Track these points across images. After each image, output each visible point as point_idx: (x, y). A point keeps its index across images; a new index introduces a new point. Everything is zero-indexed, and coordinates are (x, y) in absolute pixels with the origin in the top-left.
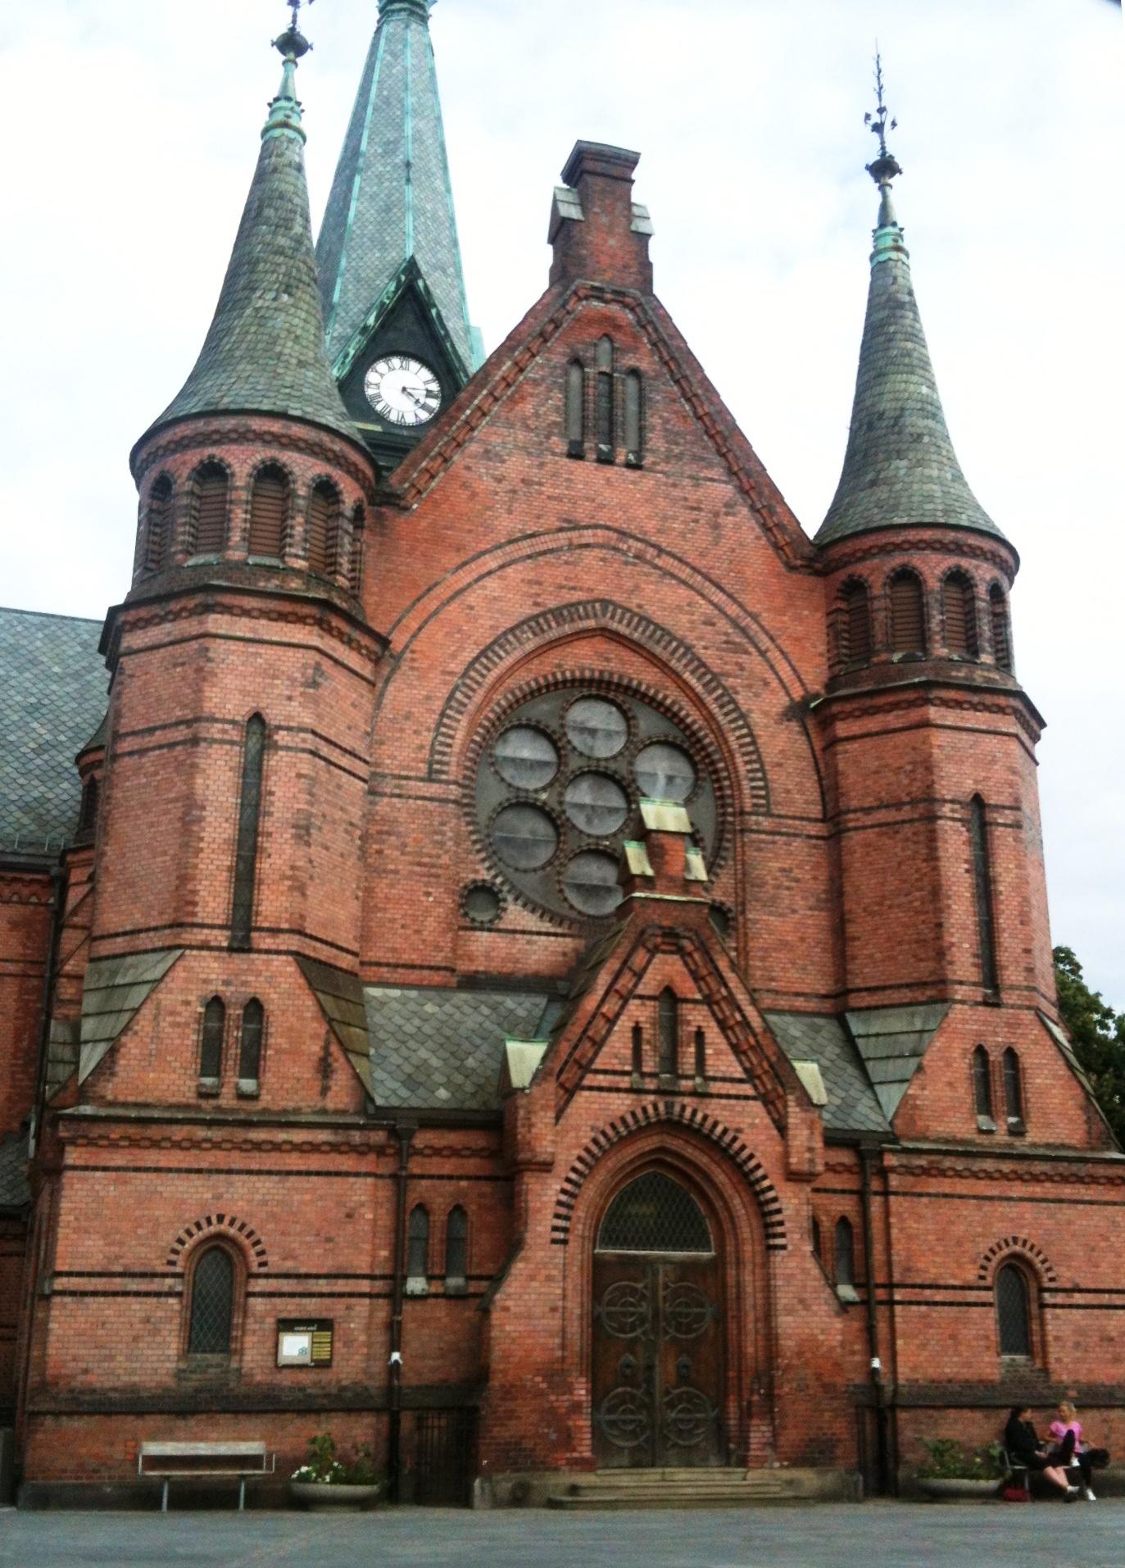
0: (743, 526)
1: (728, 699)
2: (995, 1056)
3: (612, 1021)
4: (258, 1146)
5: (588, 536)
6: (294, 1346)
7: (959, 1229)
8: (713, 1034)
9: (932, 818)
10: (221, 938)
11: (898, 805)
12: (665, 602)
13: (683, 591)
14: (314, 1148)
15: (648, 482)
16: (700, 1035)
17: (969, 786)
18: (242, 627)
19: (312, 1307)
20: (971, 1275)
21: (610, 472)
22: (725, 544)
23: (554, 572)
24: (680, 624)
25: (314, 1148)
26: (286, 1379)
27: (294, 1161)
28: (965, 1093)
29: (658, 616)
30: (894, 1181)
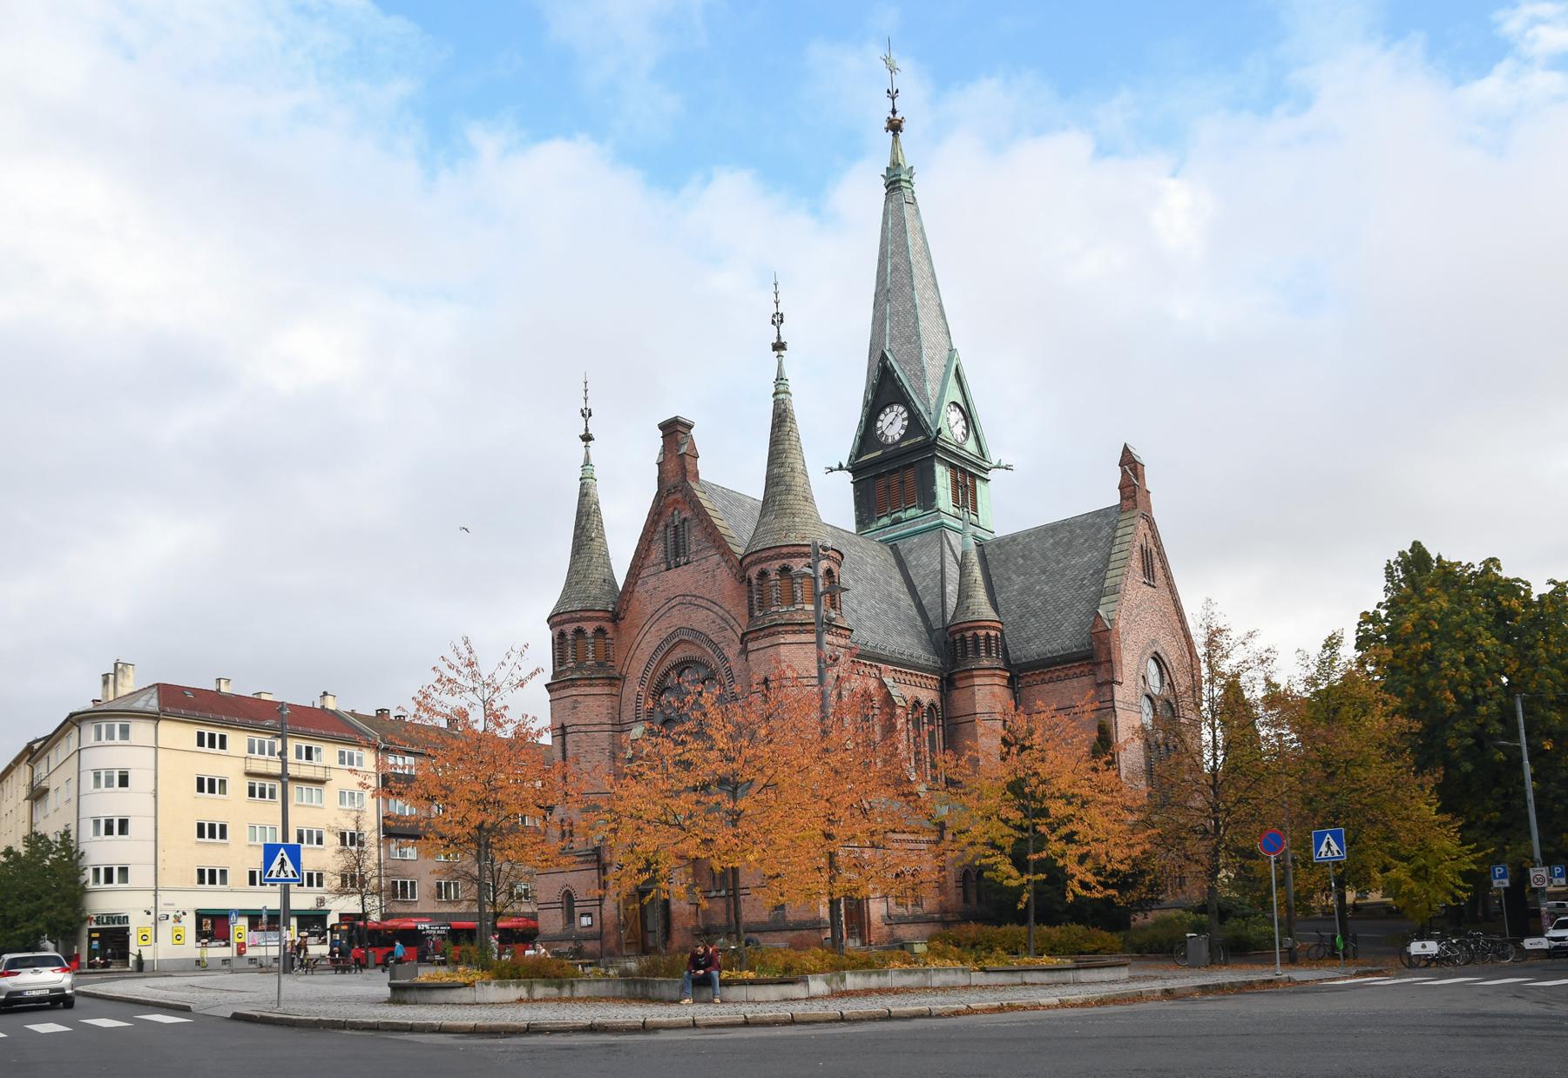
12: (700, 619)
15: (690, 568)
19: (587, 910)
23: (664, 624)
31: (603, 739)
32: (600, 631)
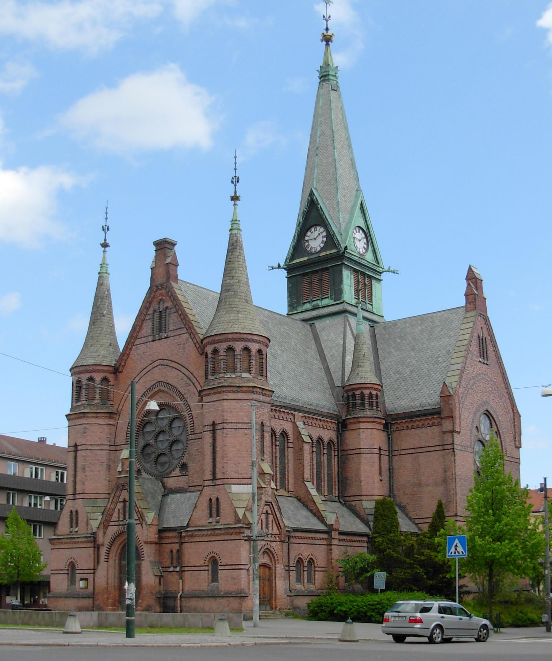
2: (214, 500)
3: (114, 509)
4: (75, 542)
5: (156, 364)
12: (173, 377)
13: (177, 371)
14: (83, 542)
19: (85, 576)
20: (202, 563)
27: (82, 545)
28: (207, 512)
31: (103, 455)
32: (105, 379)
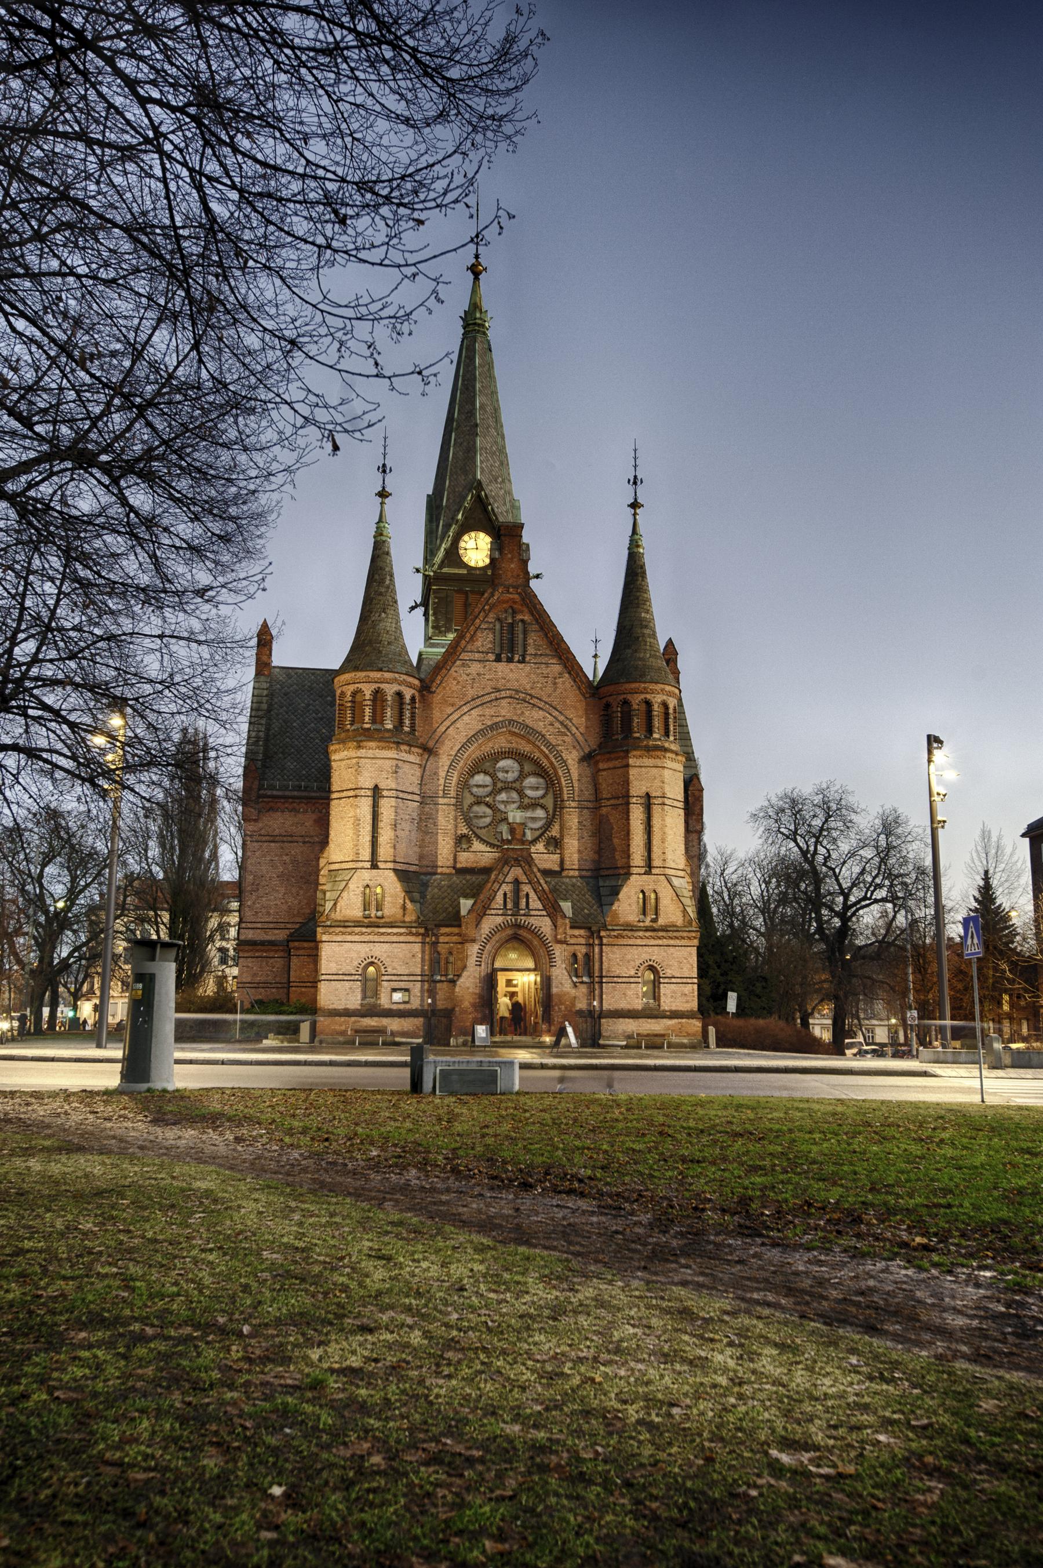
0: (566, 682)
1: (558, 755)
4: (383, 934)
5: (503, 694)
6: (397, 996)
7: (629, 957)
8: (532, 895)
9: (628, 804)
10: (368, 865)
11: (618, 798)
12: (535, 718)
14: (401, 934)
16: (527, 895)
17: (643, 790)
18: (370, 753)
19: (402, 985)
20: (632, 972)
21: (512, 666)
22: (559, 691)
23: (488, 711)
24: (540, 726)
25: (401, 934)
26: (394, 1007)
27: (395, 939)
29: (531, 724)
30: (605, 941)
32: (413, 698)
